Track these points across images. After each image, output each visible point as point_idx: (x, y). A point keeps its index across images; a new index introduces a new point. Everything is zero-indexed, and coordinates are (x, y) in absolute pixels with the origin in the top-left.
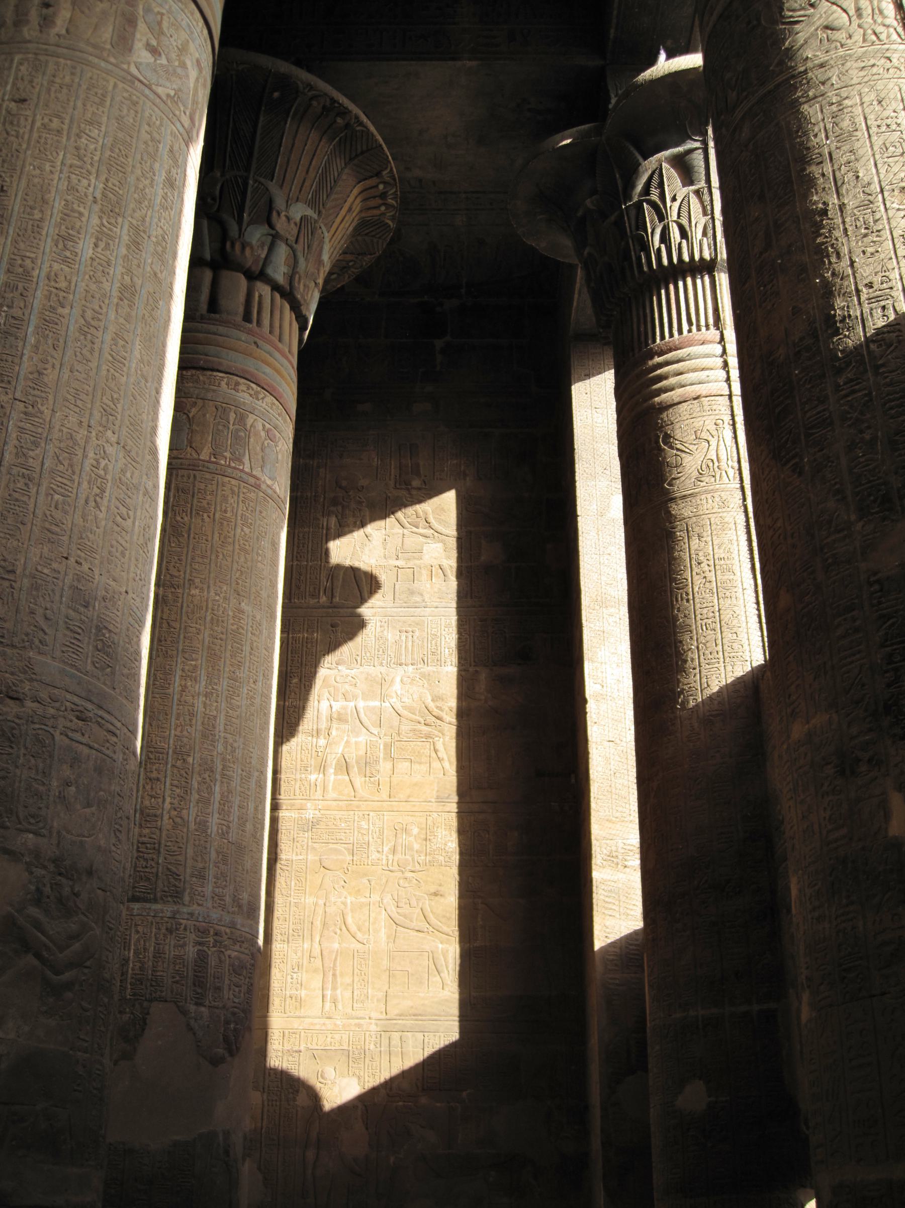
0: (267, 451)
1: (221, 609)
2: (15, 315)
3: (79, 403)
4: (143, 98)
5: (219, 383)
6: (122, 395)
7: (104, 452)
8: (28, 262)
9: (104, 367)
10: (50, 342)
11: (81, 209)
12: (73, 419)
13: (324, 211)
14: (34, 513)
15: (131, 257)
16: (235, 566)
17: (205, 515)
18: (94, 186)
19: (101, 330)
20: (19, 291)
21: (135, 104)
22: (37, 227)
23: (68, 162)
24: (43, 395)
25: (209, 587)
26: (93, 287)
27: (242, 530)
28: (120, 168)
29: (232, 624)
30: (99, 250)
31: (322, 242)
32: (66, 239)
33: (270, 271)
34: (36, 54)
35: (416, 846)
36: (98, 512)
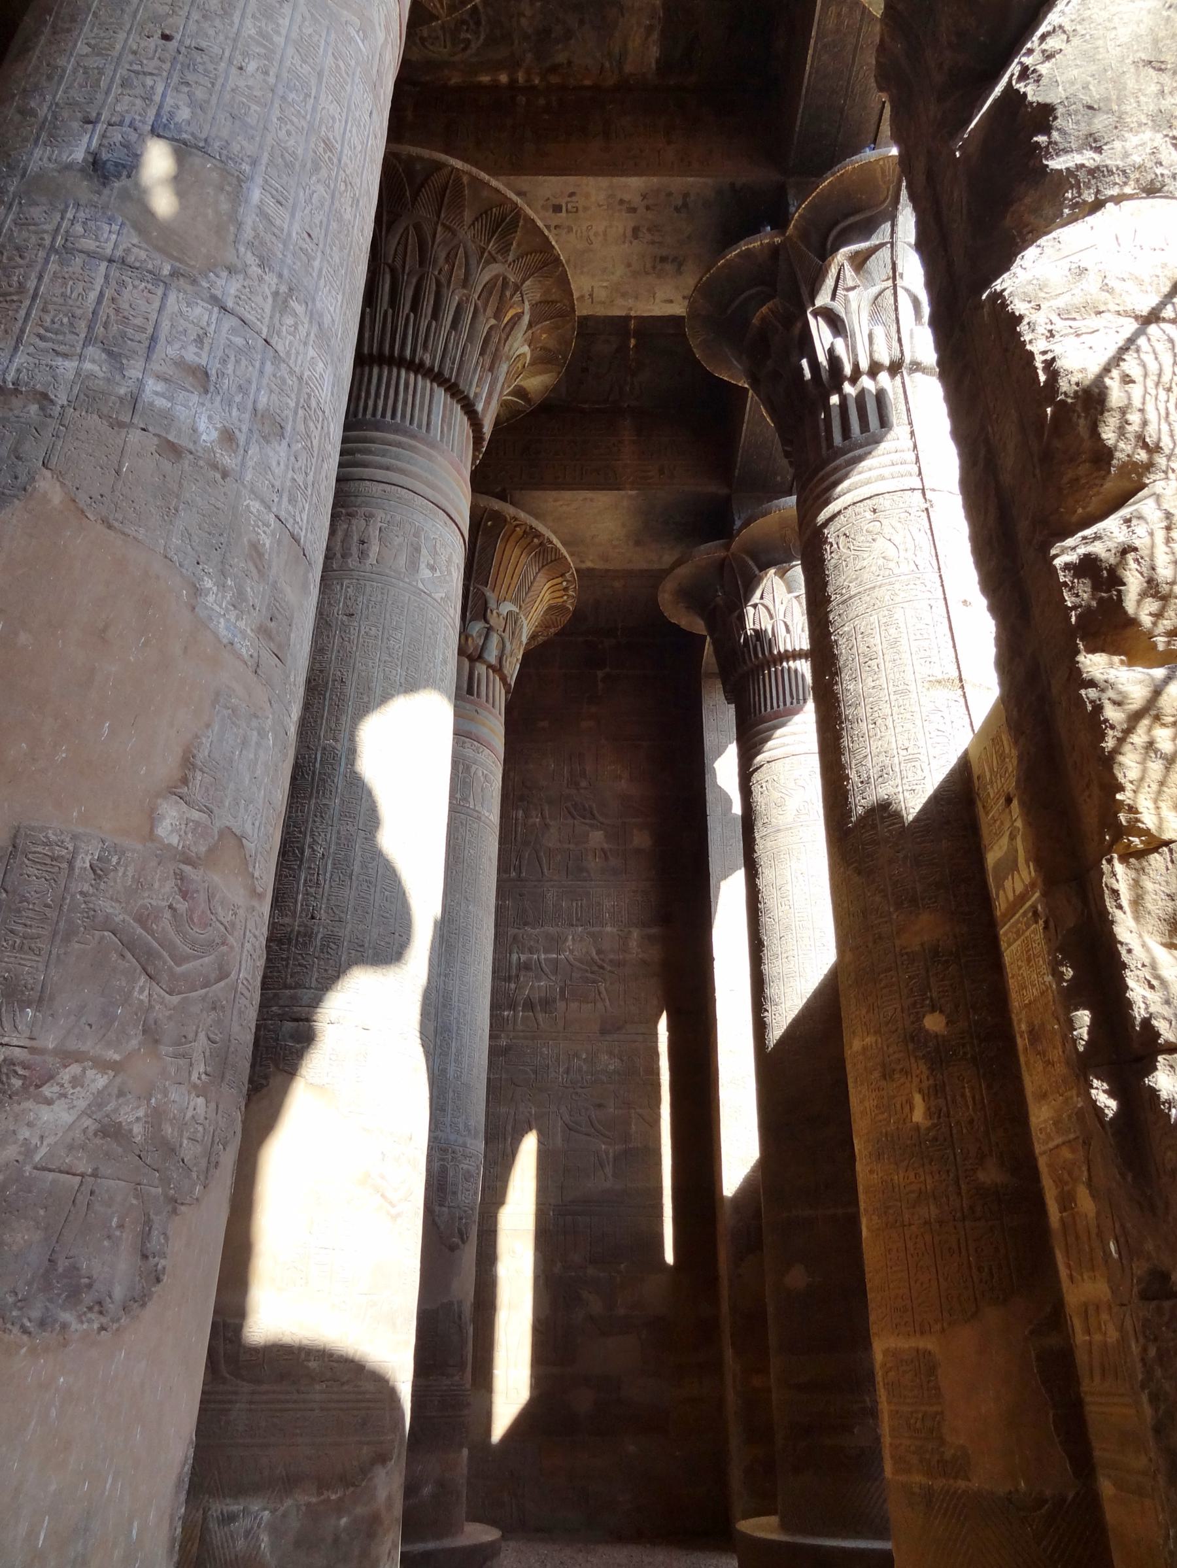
21: (422, 609)
23: (383, 659)
33: (486, 656)
35: (585, 1068)
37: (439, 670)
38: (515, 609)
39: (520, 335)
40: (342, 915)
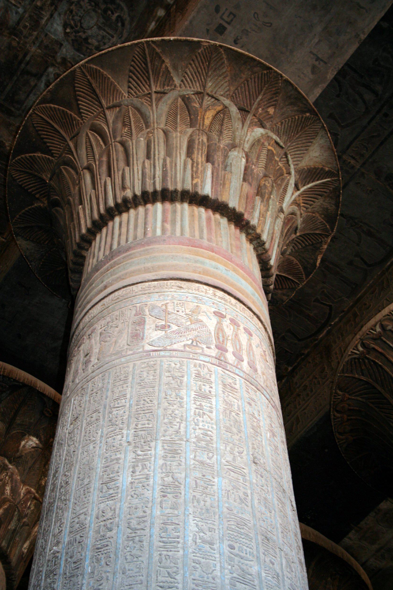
30: (138, 473)
39: (238, 124)
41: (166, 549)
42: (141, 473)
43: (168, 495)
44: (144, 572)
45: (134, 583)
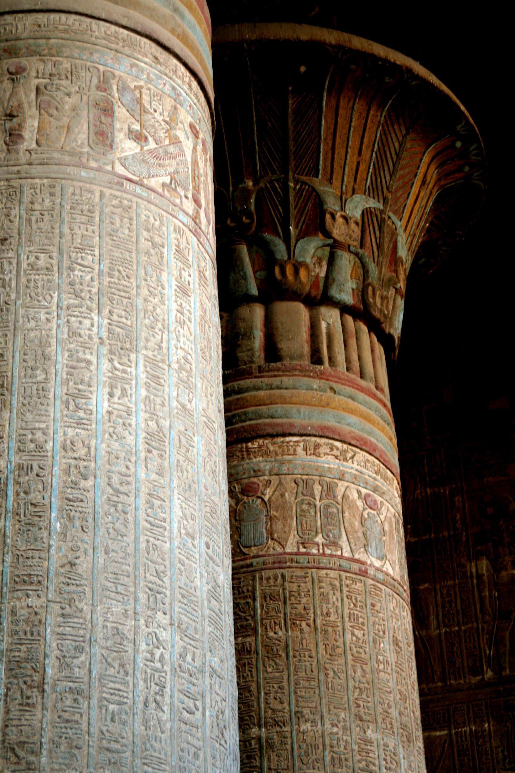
0: (368, 524)
1: (342, 744)
2: (34, 502)
3: (120, 589)
4: (135, 199)
5: (295, 450)
6: (168, 566)
7: (157, 639)
8: (39, 435)
9: (142, 539)
10: (77, 524)
11: (88, 357)
12: (118, 609)
13: (390, 196)
14: (89, 733)
15: (152, 397)
16: (351, 684)
17: (304, 624)
18: (95, 325)
19: (132, 495)
20: (35, 472)
22: (42, 390)
24: (80, 589)
25: (322, 718)
26: (116, 445)
27: (353, 634)
28: (123, 294)
29: (359, 761)
30: (116, 399)
31: (394, 234)
32: (76, 398)
33: (334, 292)
34: (7, 180)
36: (161, 714)
37: (174, 307)
38: (372, 203)
40: (32, 758)
41: (154, 536)
42: (120, 401)
43: (153, 450)
44: (131, 561)
45: (120, 572)
